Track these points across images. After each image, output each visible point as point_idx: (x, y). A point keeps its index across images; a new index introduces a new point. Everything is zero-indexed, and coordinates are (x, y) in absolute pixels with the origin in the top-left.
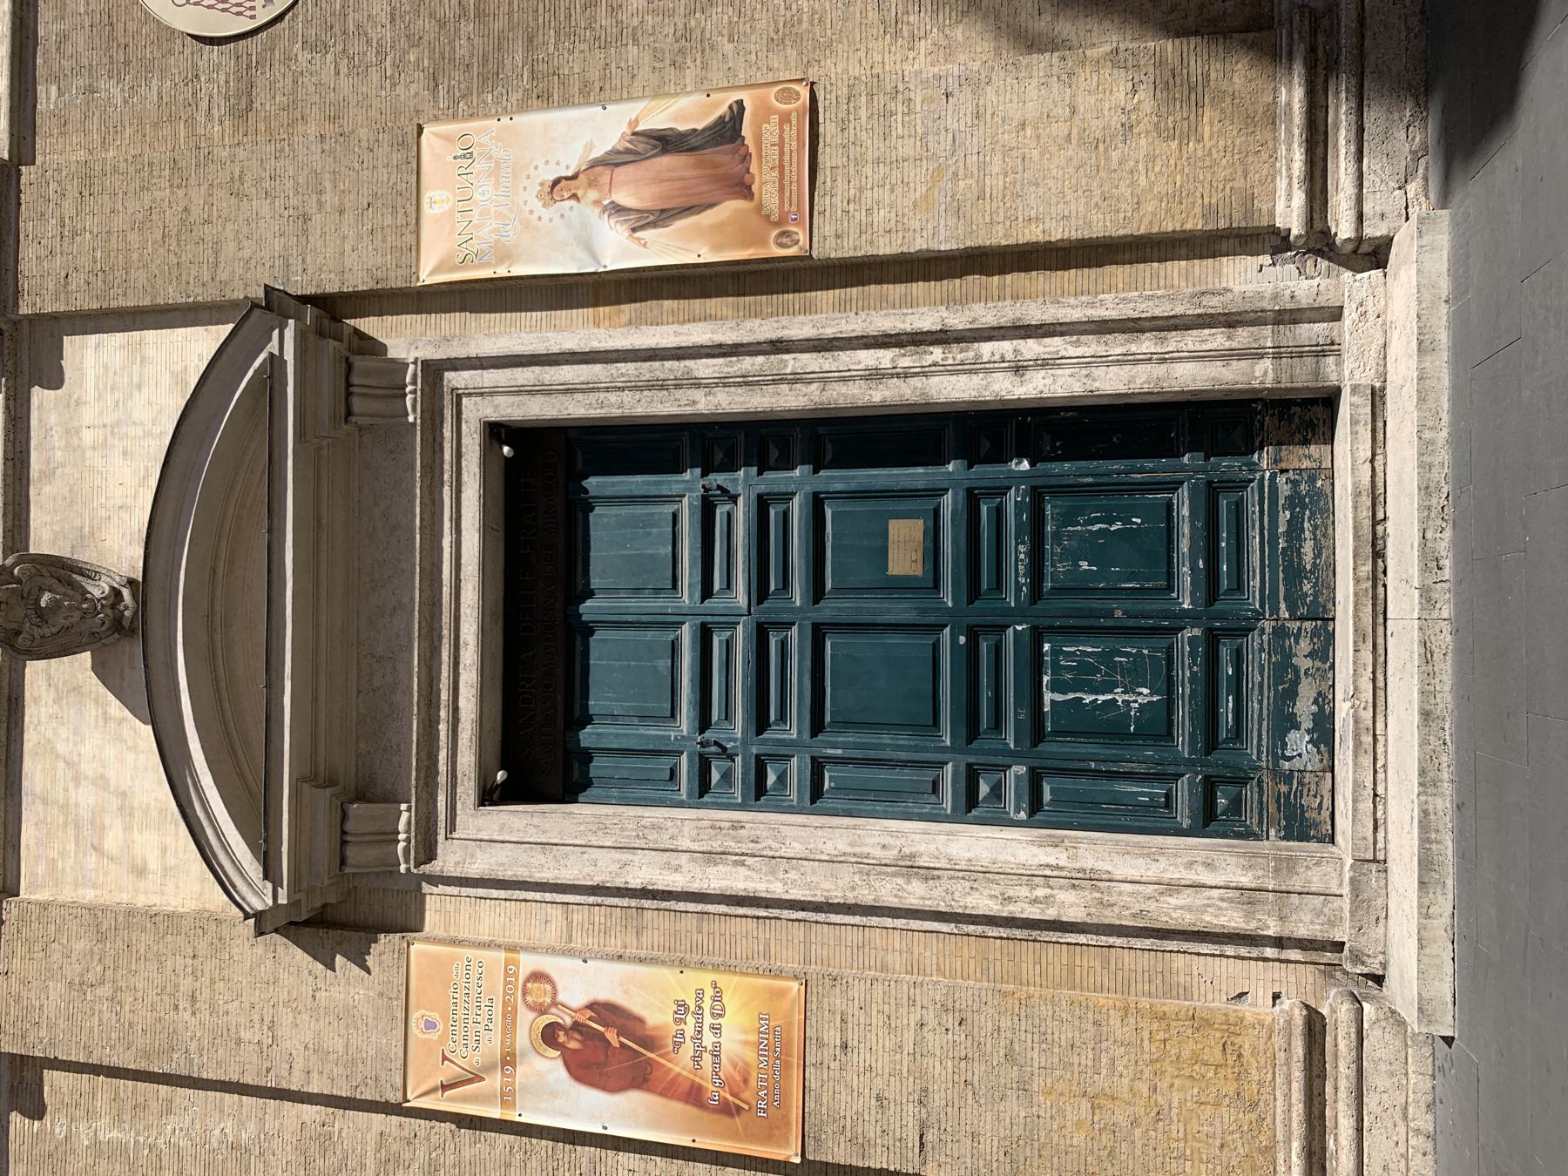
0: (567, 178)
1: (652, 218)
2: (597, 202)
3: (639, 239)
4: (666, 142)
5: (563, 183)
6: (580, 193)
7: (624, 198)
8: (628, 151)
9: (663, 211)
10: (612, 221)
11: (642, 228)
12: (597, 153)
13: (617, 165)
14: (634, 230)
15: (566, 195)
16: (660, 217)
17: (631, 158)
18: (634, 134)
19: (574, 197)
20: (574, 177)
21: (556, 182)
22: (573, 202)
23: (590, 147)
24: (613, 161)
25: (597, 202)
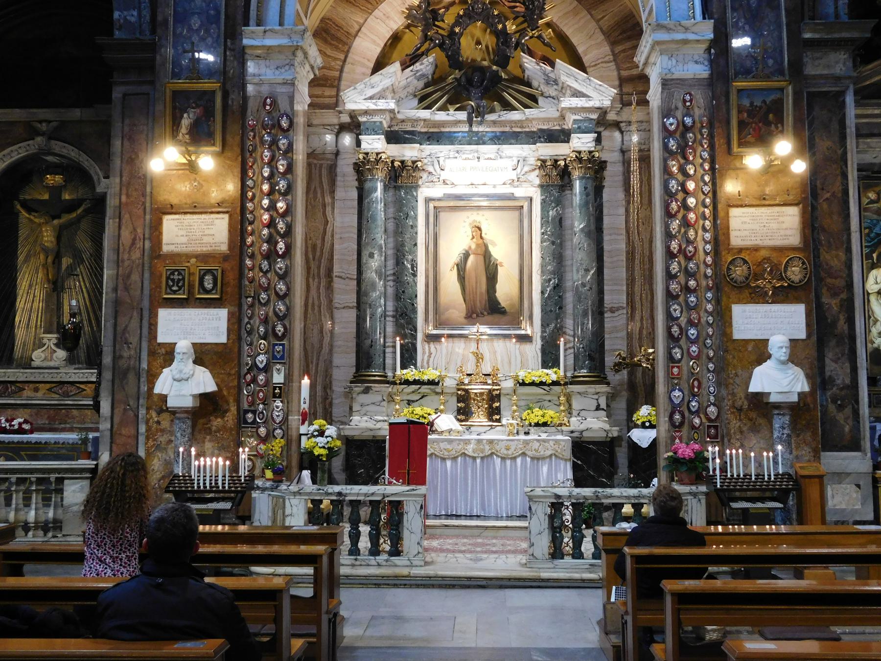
0: (481, 234)
1: (462, 273)
2: (470, 247)
3: (453, 267)
4: (492, 277)
5: (479, 232)
6: (474, 240)
7: (471, 259)
8: (490, 262)
9: (464, 278)
10: (462, 255)
11: (458, 269)
12: (491, 248)
13: (485, 257)
14: (457, 265)
15: (474, 234)
16: (462, 278)
17: (487, 263)
18: (497, 265)
19: (473, 237)
20: (481, 237)
21: (480, 229)
22: (471, 237)
23: (494, 244)
24: (486, 255)
25: (470, 247)
